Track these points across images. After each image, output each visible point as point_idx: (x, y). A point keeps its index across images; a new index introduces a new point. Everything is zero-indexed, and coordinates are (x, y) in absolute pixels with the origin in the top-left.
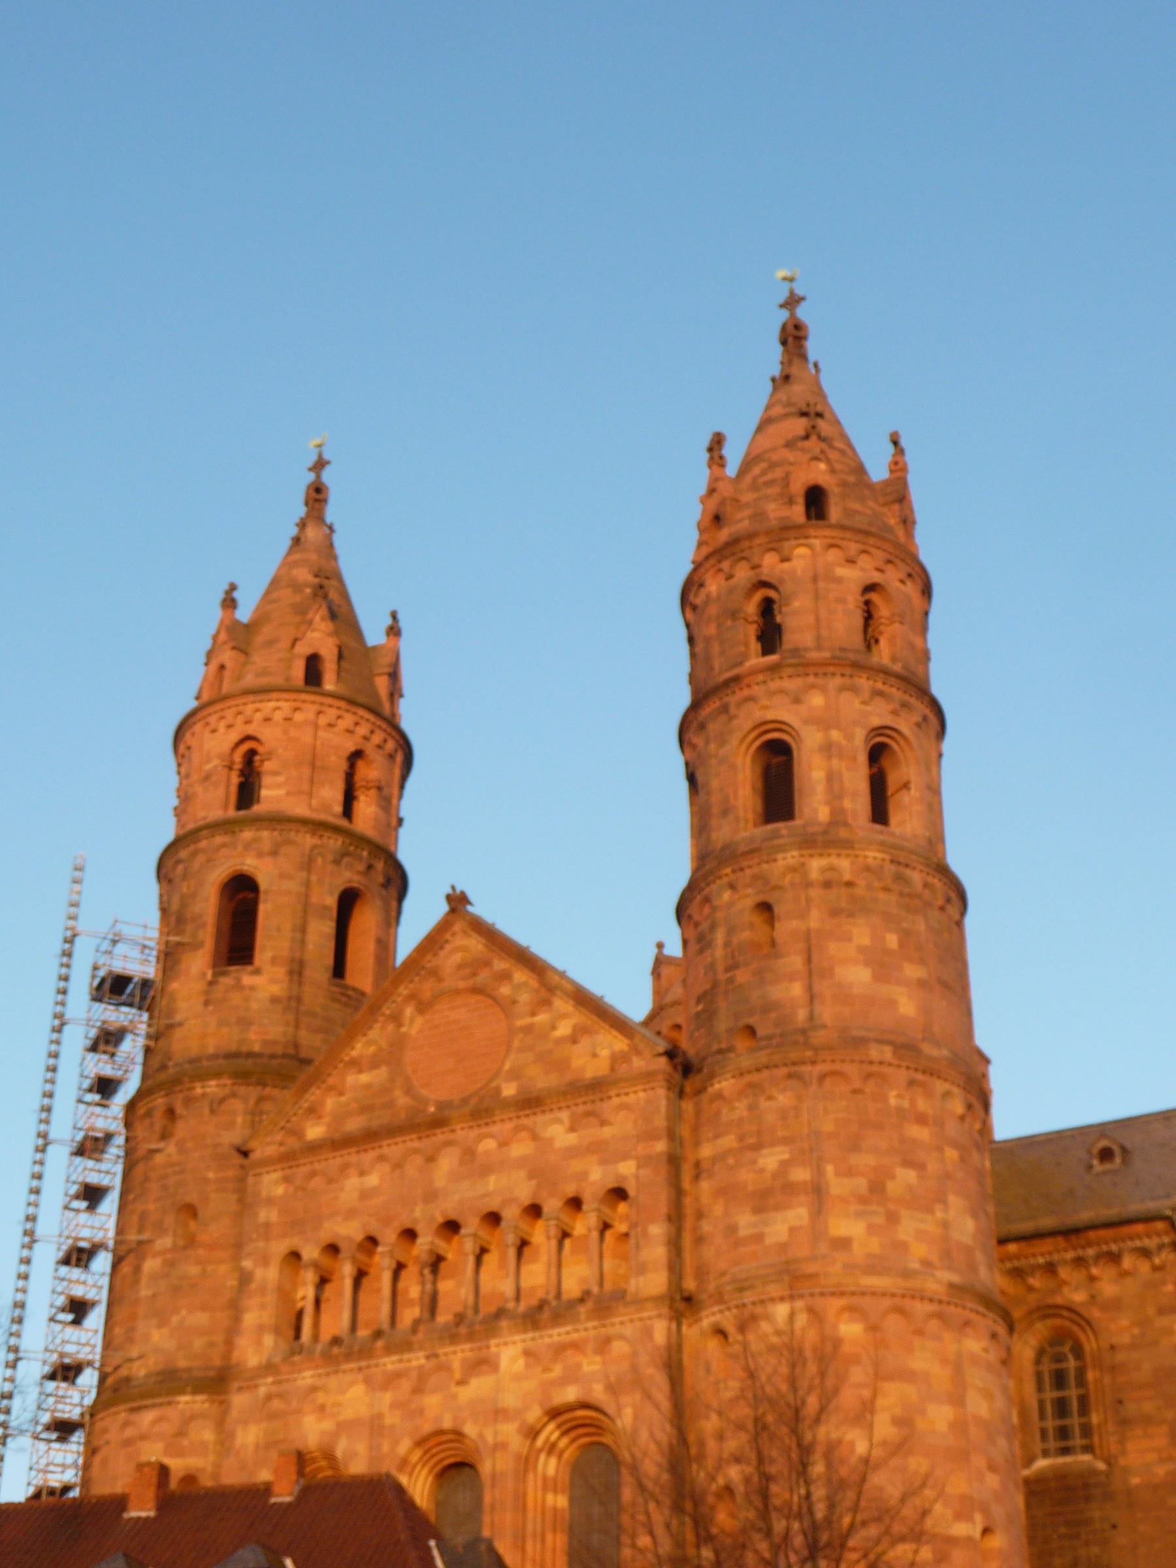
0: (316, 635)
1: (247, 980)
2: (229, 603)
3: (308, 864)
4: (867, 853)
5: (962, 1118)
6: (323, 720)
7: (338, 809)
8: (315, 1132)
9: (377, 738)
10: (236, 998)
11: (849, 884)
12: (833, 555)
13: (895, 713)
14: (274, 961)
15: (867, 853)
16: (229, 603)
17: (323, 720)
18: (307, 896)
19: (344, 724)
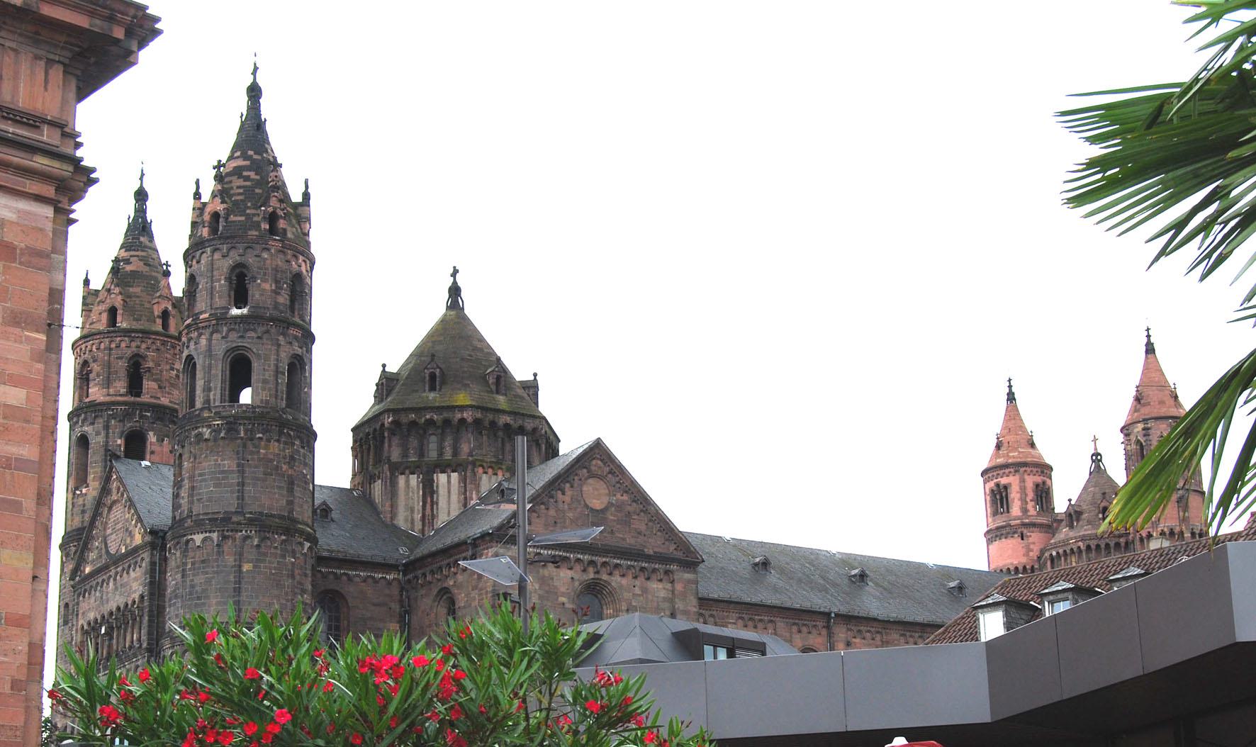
0: (113, 296)
1: (84, 491)
2: (87, 282)
3: (107, 427)
4: (214, 423)
5: (258, 546)
6: (113, 346)
7: (123, 391)
8: (88, 570)
9: (144, 346)
10: (80, 501)
11: (206, 440)
12: (217, 256)
13: (242, 337)
14: (94, 480)
15: (214, 423)
16: (87, 282)
17: (113, 346)
18: (107, 442)
19: (123, 345)
